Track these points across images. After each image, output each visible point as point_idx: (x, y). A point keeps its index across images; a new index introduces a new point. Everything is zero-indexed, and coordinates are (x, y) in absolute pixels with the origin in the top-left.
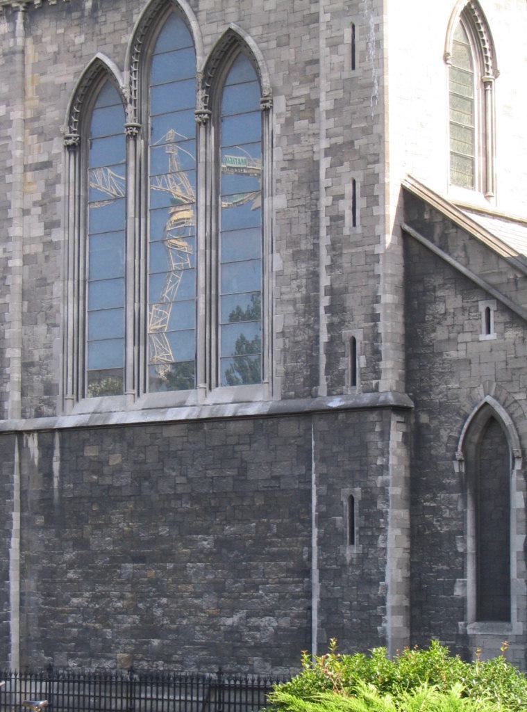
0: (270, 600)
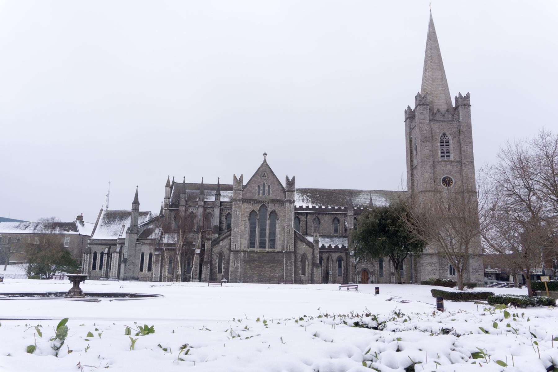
0: (277, 272)
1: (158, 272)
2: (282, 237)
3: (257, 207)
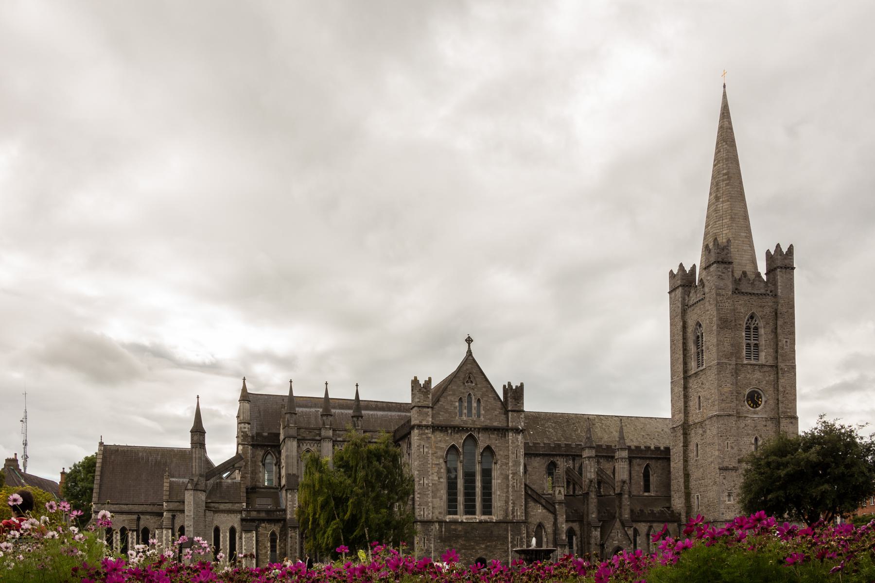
2: (504, 495)
3: (459, 440)
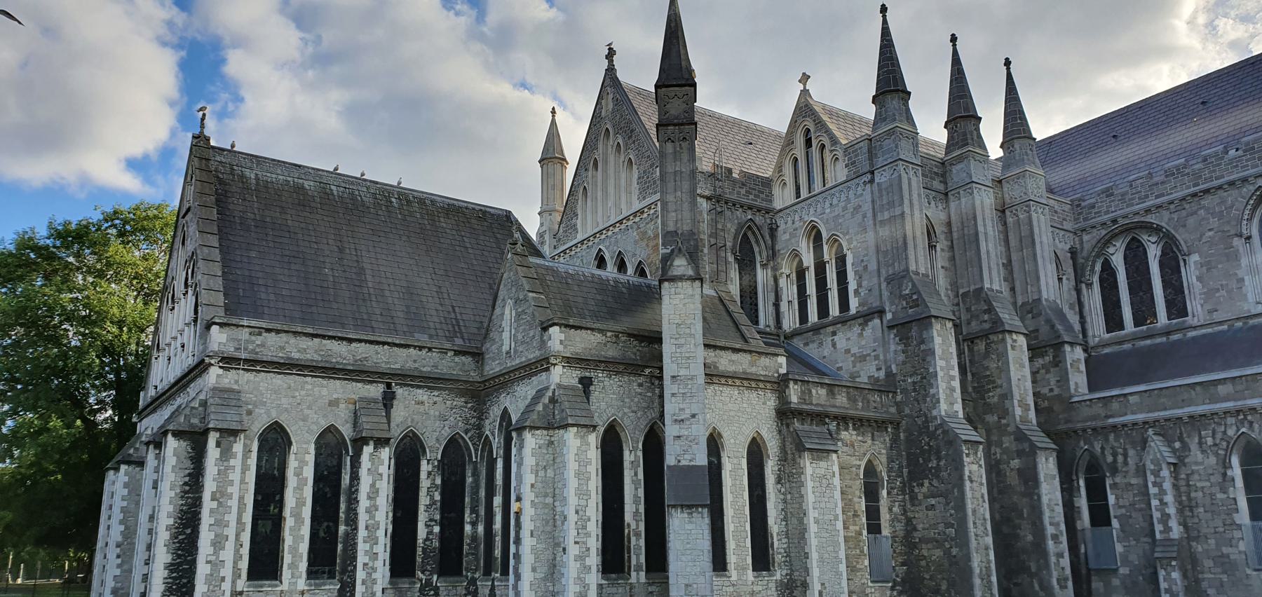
1: (838, 574)
